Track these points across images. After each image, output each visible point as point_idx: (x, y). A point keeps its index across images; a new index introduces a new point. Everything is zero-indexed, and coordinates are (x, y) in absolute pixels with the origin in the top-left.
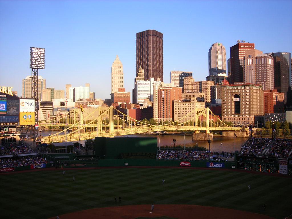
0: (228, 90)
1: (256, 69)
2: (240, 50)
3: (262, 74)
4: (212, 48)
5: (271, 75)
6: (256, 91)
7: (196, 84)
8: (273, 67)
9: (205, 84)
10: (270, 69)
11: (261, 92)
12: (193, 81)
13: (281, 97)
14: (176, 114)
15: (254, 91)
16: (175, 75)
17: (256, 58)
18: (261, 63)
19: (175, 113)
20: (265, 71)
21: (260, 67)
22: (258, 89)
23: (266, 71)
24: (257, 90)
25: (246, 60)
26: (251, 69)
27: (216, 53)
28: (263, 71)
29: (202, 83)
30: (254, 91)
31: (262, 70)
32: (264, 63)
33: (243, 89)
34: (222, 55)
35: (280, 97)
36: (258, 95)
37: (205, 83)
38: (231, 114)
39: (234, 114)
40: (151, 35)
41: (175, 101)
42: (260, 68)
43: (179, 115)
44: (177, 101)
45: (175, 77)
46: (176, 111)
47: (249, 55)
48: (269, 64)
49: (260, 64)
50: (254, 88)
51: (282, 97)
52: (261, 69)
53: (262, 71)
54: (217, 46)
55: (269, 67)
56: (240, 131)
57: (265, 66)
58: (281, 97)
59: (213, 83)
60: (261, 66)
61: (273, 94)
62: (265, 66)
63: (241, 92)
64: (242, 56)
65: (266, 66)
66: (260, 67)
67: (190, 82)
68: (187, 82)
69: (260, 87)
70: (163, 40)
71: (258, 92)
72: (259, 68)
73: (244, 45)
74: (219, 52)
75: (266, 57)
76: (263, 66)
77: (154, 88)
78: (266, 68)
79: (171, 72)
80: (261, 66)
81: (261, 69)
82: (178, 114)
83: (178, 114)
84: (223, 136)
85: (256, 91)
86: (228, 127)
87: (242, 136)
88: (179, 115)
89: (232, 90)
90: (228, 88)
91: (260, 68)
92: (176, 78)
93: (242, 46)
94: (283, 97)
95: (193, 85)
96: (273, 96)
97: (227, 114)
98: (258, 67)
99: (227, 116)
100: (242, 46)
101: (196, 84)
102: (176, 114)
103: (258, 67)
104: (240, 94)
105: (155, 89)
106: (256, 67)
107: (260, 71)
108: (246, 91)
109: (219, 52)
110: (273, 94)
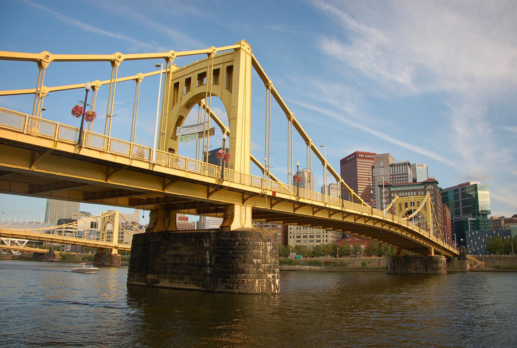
2: (358, 160)
14: (292, 237)
17: (391, 166)
18: (401, 173)
19: (291, 235)
32: (404, 173)
43: (299, 239)
49: (397, 175)
66: (398, 178)
73: (364, 154)
80: (400, 178)
82: (295, 237)
83: (295, 237)
88: (299, 239)
90: (392, 189)
102: (292, 237)
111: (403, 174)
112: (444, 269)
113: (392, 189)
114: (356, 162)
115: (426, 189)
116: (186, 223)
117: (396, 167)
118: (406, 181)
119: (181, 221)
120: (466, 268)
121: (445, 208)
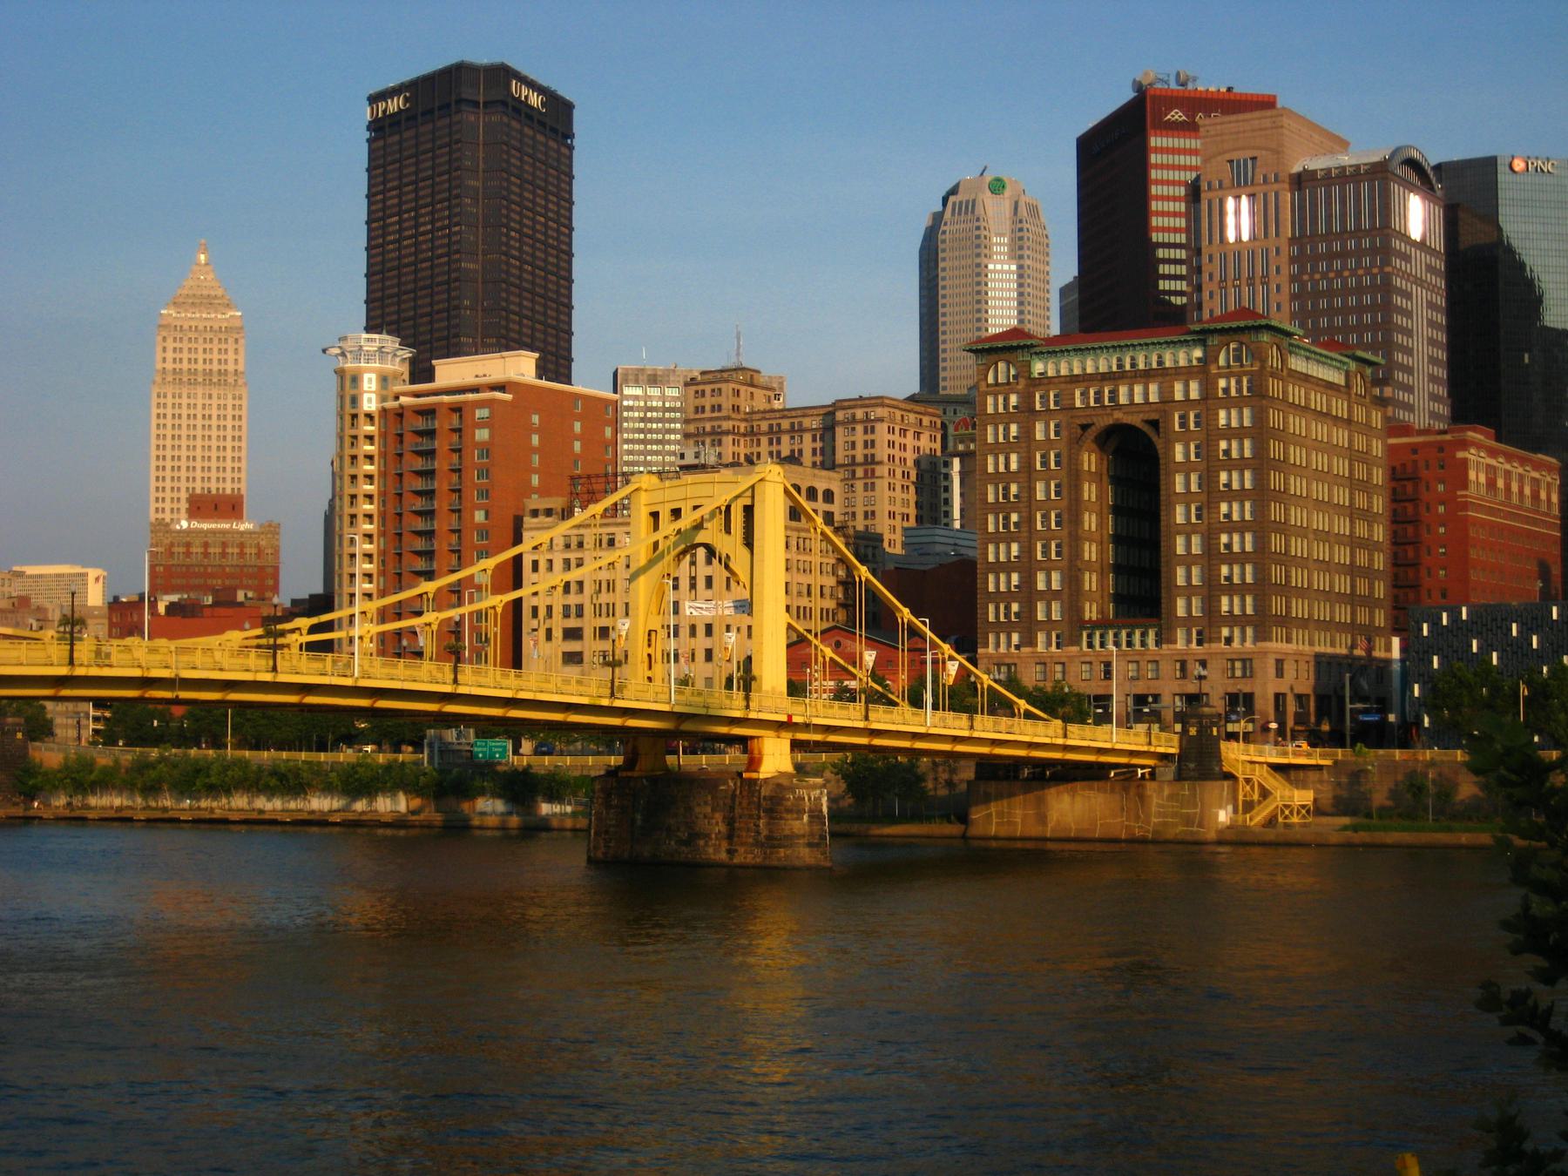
0: (1044, 380)
1: (1293, 279)
2: (1154, 141)
3: (1353, 320)
4: (948, 214)
5: (1428, 332)
6: (1318, 400)
7: (785, 424)
8: (1440, 265)
9: (860, 428)
10: (1419, 282)
11: (1359, 414)
12: (760, 403)
13: (1535, 496)
15: (1296, 394)
16: (647, 398)
17: (1301, 181)
20: (1373, 288)
21: (1331, 256)
22: (1337, 378)
23: (1387, 288)
24: (1330, 386)
25: (1204, 206)
26: (1251, 281)
27: (978, 247)
28: (1360, 290)
29: (840, 416)
30: (1296, 394)
31: (1352, 282)
33: (1185, 373)
34: (1020, 267)
35: (1527, 491)
36: (1341, 436)
37: (860, 414)
38: (1074, 628)
39: (1095, 625)
40: (476, 104)
41: (535, 513)
42: (1330, 267)
43: (573, 646)
44: (549, 512)
45: (652, 409)
46: (542, 612)
47: (1235, 156)
48: (1405, 238)
49: (1329, 236)
50: (1297, 364)
51: (1543, 495)
52: (1339, 274)
53: (1346, 292)
54: (987, 198)
55: (1406, 258)
56: (1169, 772)
57: (1373, 251)
58: (1535, 496)
59: (926, 421)
60: (1344, 255)
61: (1471, 455)
62: (1373, 251)
63: (1167, 400)
64: (1180, 168)
65: (1386, 252)
66: (1331, 256)
67: (736, 409)
68: (708, 414)
69: (1353, 366)
70: (571, 148)
71: (1340, 407)
72: (1323, 266)
74: (1000, 244)
75: (1379, 172)
76: (1359, 253)
77: (349, 391)
78: (1386, 262)
79: (615, 374)
80: (1344, 255)
81: (1339, 274)
82: (558, 634)
84: (975, 831)
85: (1318, 400)
86: (1028, 715)
87: (1188, 820)
88: (573, 646)
89: (1074, 380)
90: (1038, 367)
91: (1330, 267)
92: (658, 420)
93: (1176, 115)
94: (1555, 498)
95: (764, 440)
96: (1472, 475)
97: (1028, 627)
98: (1316, 258)
99: (1033, 643)
100: (1176, 115)
101: (785, 424)
103: (1316, 258)
104: (1154, 424)
105: (355, 401)
106: (1292, 260)
107: (1330, 293)
108: (1222, 383)
109: (1000, 244)
110: (1471, 455)
111: (1358, 233)
112: (810, 845)
113: (1038, 367)
114: (1143, 151)
115: (1214, 371)
116: (223, 532)
117: (1321, 192)
118: (1374, 277)
119: (195, 524)
120: (1201, 825)
121: (1460, 455)
